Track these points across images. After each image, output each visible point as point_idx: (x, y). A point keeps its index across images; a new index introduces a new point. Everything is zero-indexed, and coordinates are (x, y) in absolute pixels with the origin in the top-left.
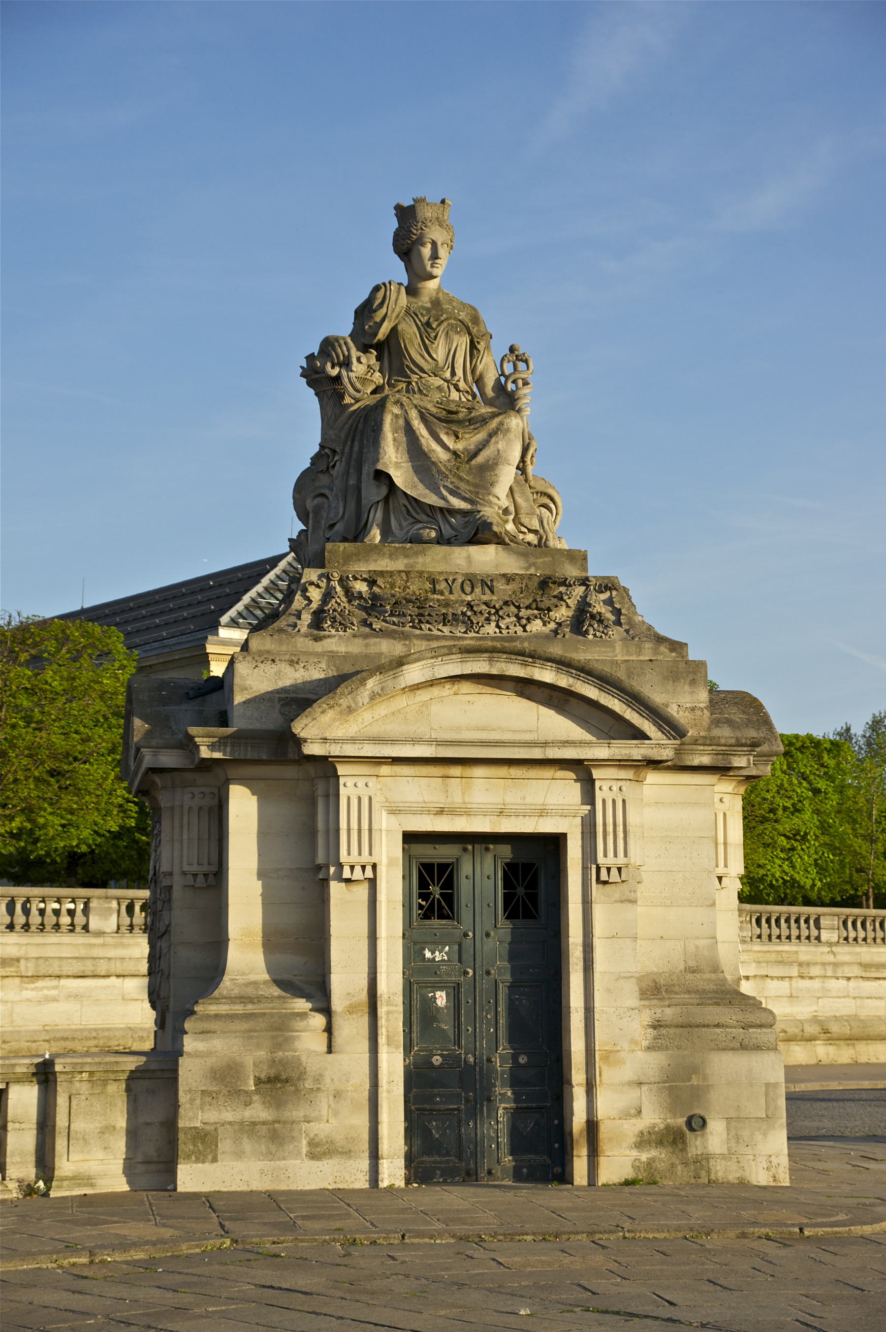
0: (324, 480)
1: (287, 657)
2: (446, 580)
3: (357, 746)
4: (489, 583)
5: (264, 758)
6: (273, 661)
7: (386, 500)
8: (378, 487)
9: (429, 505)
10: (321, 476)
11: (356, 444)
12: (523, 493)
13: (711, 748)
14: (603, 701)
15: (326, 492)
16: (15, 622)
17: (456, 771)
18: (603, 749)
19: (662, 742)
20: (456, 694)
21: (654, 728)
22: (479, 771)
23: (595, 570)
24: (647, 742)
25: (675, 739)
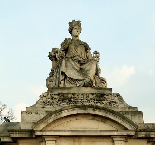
0: (52, 78)
1: (35, 112)
2: (77, 95)
3: (49, 133)
4: (88, 95)
5: (27, 137)
6: (31, 113)
7: (64, 79)
8: (63, 76)
9: (74, 79)
10: (51, 77)
11: (59, 69)
12: (98, 80)
13: (145, 133)
14: (122, 123)
15: (52, 80)
16: (51, 126)
17: (77, 139)
18: (116, 132)
19: (131, 130)
20: (77, 119)
21: (129, 126)
22: (83, 139)
23: (114, 92)
24: (127, 130)
25: (135, 129)
